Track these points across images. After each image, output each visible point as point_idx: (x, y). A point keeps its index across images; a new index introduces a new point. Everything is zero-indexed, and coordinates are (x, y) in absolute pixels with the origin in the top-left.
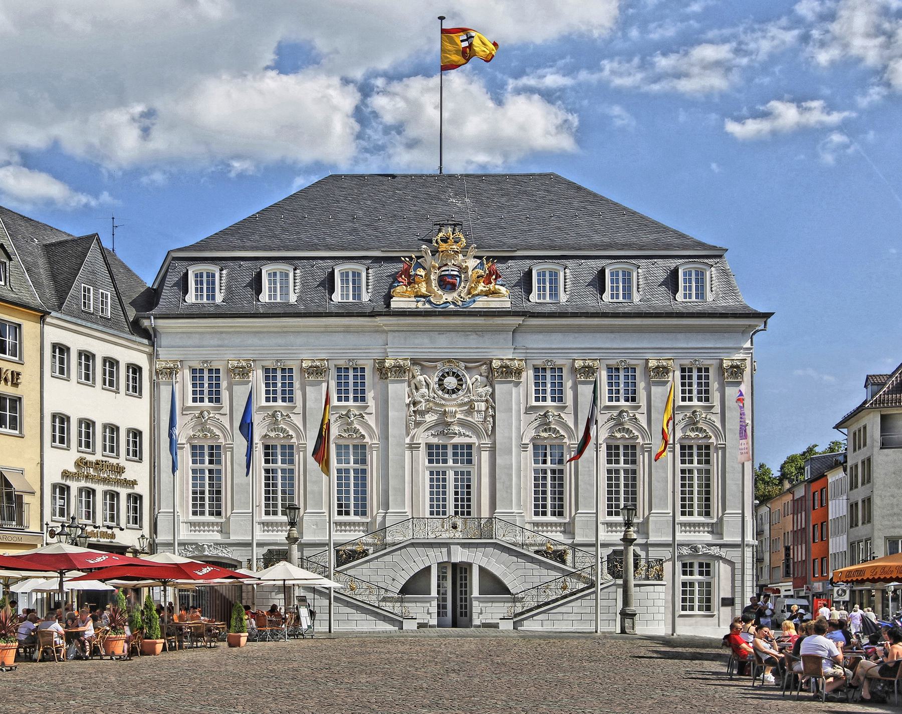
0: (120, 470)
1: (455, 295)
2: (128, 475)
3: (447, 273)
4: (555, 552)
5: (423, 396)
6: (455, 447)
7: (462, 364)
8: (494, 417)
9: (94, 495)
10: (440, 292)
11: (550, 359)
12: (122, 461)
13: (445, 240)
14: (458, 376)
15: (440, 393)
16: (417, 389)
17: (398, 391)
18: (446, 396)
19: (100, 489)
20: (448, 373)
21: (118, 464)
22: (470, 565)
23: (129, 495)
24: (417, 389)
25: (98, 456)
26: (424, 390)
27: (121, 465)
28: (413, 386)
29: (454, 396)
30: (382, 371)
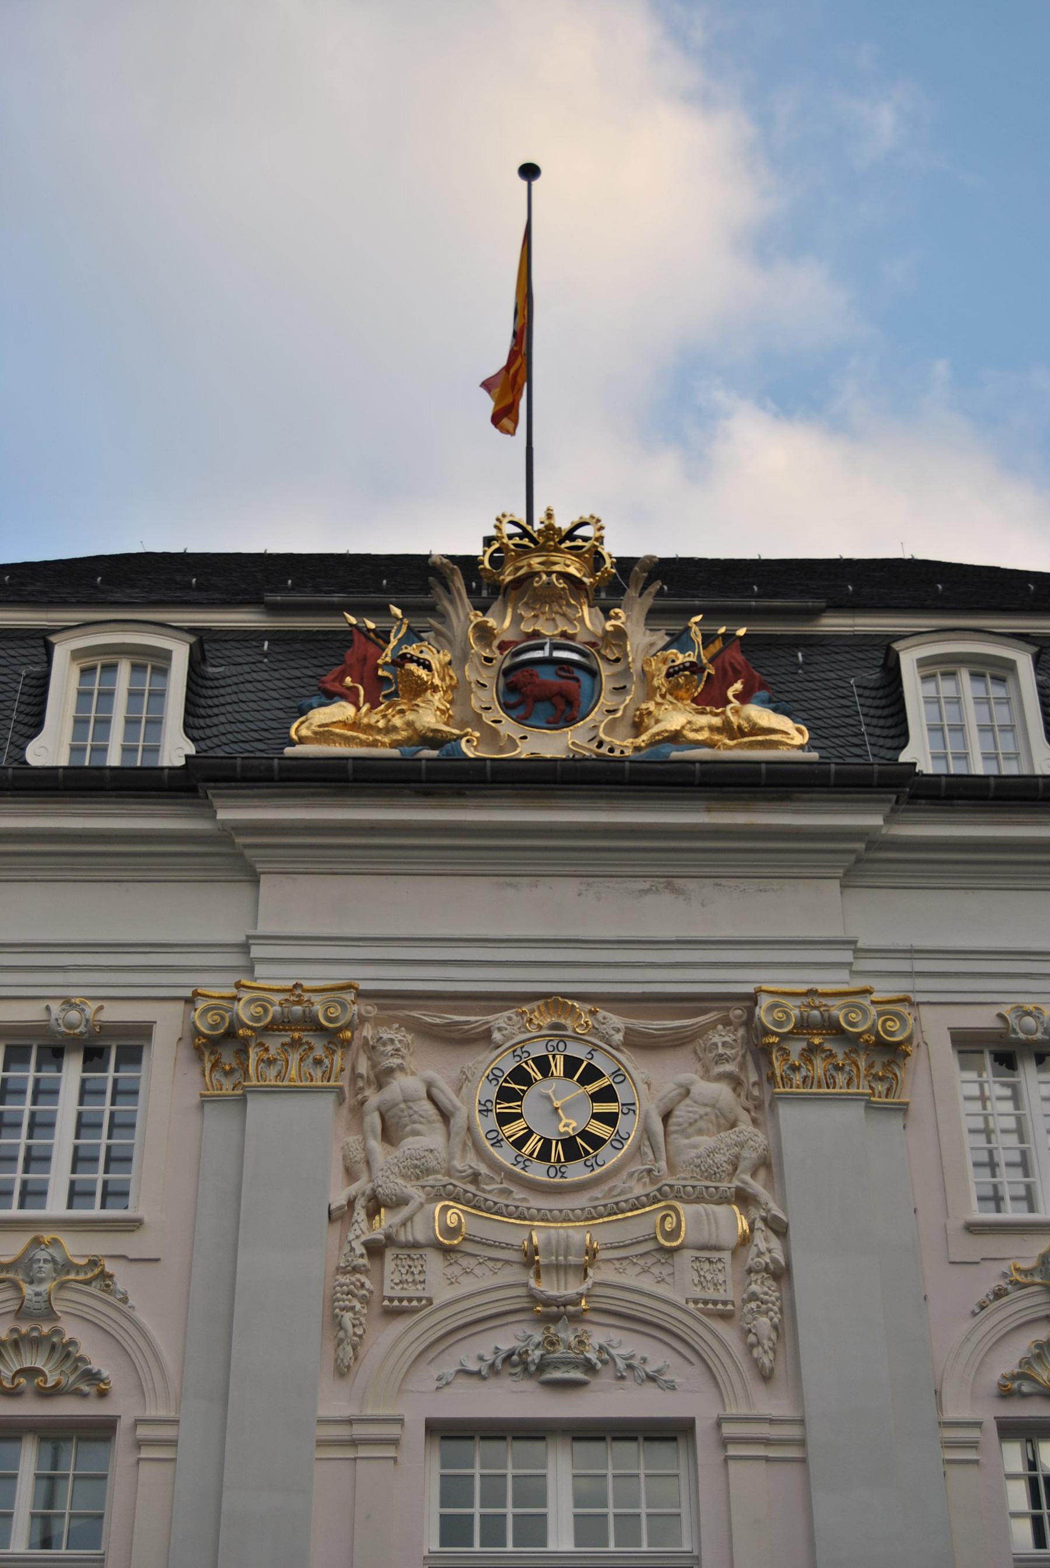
5: (420, 1171)
7: (615, 1022)
8: (781, 1274)
10: (508, 727)
11: (1029, 1002)
14: (592, 1074)
15: (505, 1156)
16: (389, 1134)
17: (297, 1130)
18: (537, 1172)
20: (543, 1064)
24: (389, 1134)
26: (427, 1140)
28: (374, 1120)
29: (577, 1172)
30: (221, 1045)
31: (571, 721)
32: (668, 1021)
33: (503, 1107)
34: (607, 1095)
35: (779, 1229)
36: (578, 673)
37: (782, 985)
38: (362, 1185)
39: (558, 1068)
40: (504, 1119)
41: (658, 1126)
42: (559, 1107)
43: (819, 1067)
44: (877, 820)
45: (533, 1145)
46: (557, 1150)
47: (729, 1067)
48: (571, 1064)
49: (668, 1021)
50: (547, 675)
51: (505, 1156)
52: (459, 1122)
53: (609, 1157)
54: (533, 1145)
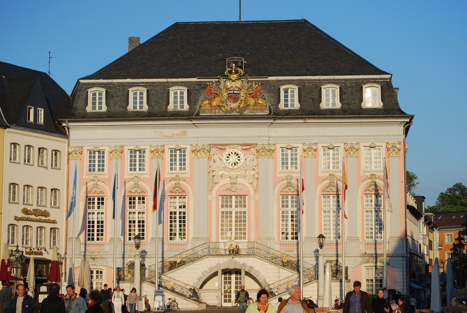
0: (46, 214)
1: (237, 104)
2: (51, 218)
3: (232, 92)
4: (288, 262)
6: (236, 196)
7: (240, 147)
9: (32, 230)
12: (48, 209)
13: (230, 72)
14: (237, 154)
16: (214, 162)
19: (35, 225)
21: (45, 211)
22: (241, 270)
23: (51, 229)
25: (35, 207)
27: (47, 211)
29: (235, 167)
31: (237, 102)
32: (247, 146)
33: (227, 159)
34: (239, 157)
35: (258, 174)
36: (237, 95)
37: (260, 143)
38: (211, 169)
39: (233, 153)
40: (227, 160)
41: (245, 161)
42: (233, 158)
43: (263, 154)
44: (272, 122)
45: (231, 164)
46: (233, 164)
47: (254, 153)
48: (235, 153)
49: (247, 146)
50: (233, 95)
51: (227, 165)
52: (222, 161)
53: (239, 165)
54: (231, 164)
